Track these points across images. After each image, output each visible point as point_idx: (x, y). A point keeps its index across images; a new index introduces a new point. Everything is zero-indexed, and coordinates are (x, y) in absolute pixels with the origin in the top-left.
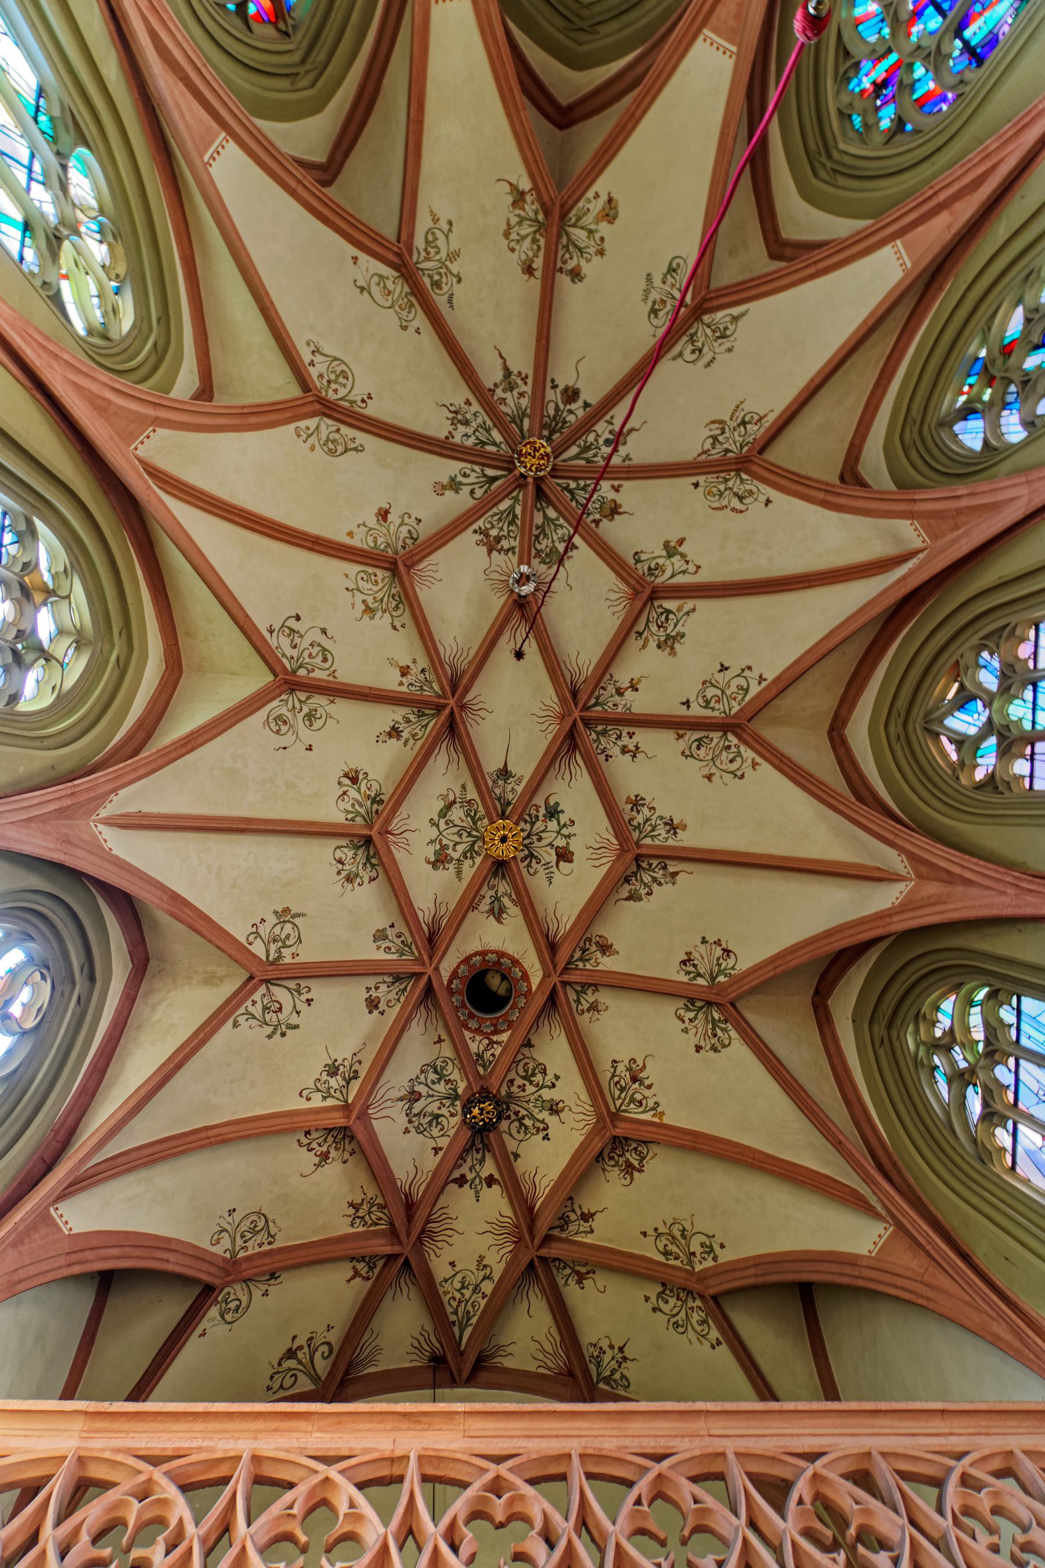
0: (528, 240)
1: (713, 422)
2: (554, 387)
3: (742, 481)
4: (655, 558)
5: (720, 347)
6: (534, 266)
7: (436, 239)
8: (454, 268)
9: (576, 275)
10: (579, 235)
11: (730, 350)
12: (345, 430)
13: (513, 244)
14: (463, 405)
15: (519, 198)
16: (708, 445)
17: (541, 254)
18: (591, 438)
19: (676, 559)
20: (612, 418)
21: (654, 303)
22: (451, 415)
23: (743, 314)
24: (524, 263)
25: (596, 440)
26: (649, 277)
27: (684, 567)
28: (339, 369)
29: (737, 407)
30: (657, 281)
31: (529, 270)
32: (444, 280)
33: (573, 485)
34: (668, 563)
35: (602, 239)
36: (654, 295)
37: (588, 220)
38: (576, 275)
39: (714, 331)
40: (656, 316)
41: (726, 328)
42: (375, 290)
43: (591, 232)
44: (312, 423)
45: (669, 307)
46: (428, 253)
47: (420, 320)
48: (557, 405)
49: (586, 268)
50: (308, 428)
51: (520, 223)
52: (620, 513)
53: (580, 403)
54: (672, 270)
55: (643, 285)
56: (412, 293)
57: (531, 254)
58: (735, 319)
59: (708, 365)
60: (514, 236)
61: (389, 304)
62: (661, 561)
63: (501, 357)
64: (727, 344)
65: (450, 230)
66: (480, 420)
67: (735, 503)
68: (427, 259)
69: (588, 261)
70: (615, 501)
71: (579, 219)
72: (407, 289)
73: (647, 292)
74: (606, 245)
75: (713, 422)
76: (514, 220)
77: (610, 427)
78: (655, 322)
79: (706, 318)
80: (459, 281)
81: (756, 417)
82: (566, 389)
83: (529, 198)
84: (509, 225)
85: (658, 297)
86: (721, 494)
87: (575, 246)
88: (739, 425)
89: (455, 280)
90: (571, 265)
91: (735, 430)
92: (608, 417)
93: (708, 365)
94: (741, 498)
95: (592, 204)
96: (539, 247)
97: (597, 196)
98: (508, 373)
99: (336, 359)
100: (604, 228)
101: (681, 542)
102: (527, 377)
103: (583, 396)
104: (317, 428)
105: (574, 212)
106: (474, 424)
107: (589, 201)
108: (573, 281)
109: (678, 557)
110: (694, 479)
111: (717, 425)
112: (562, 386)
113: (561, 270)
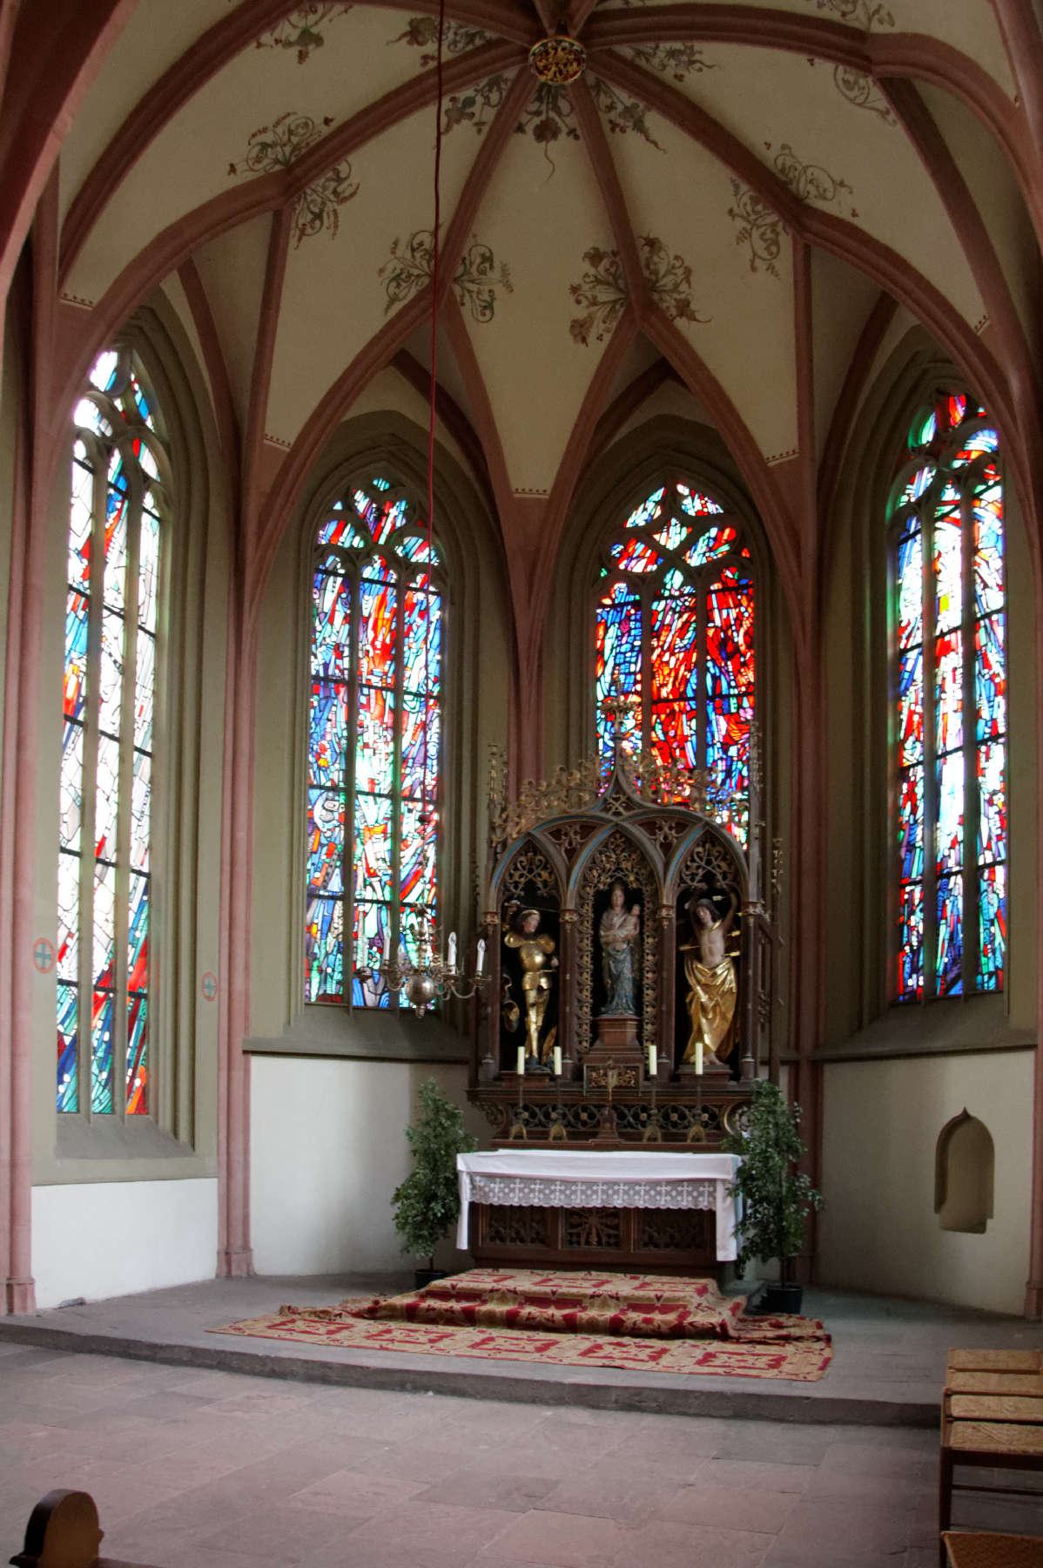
0: (662, 272)
1: (352, 195)
2: (572, 132)
3: (277, 161)
4: (323, 17)
5: (393, 266)
6: (647, 249)
7: (767, 248)
8: (740, 224)
9: (595, 257)
10: (605, 295)
11: (381, 271)
12: (836, 16)
13: (678, 264)
14: (686, 73)
15: (684, 308)
16: (343, 168)
17: (643, 262)
18: (494, 97)
19: (294, 35)
20: (479, 131)
21: (492, 267)
22: (697, 57)
23: (388, 308)
24: (660, 249)
25: (487, 98)
26: (509, 288)
27: (277, 34)
28: (855, 92)
29: (336, 227)
30: (499, 290)
31: (652, 243)
32: (749, 208)
33: (488, 34)
34: (302, 24)
35: (578, 302)
36: (495, 275)
37: (600, 313)
38: (595, 257)
39: (410, 275)
40: (483, 256)
41: (398, 286)
42: (828, 184)
43: (594, 303)
44: (876, 28)
45: (474, 269)
46: (773, 231)
47: (770, 157)
48: (559, 114)
49: (587, 267)
50: (881, 22)
51: (676, 286)
52: (405, 35)
53: (530, 128)
54: (489, 306)
55: (512, 280)
56: (785, 183)
57: (656, 259)
58: (393, 300)
59: (396, 243)
60: (680, 272)
61: (809, 171)
62: (312, 18)
63: (656, 144)
64: (388, 274)
65: (753, 261)
66: (656, 61)
67: (268, 138)
68: (774, 225)
69: (586, 275)
70: (421, 44)
71: (613, 310)
72: (793, 187)
73: (505, 271)
74: (572, 299)
75: (352, 195)
76: (684, 287)
77: (476, 119)
78: (482, 250)
79: (426, 281)
80: (731, 211)
81: (309, 231)
82: (555, 135)
83: (674, 311)
84: (688, 282)
85: (490, 274)
86: (291, 132)
87: (609, 284)
88: (322, 211)
89: (736, 210)
90: (605, 263)
91: (324, 203)
92: (486, 129)
93: (396, 243)
94: (264, 146)
95: (601, 335)
96: (648, 266)
97: (600, 338)
98: (639, 126)
99: (860, 105)
100: (581, 313)
101: (302, 56)
102: (613, 130)
103: (529, 135)
104: (870, 20)
105: (620, 314)
106: (661, 54)
107: (608, 330)
108: (596, 250)
109: (293, 39)
110: (334, 125)
111: (347, 194)
112: (562, 136)
113: (614, 254)
